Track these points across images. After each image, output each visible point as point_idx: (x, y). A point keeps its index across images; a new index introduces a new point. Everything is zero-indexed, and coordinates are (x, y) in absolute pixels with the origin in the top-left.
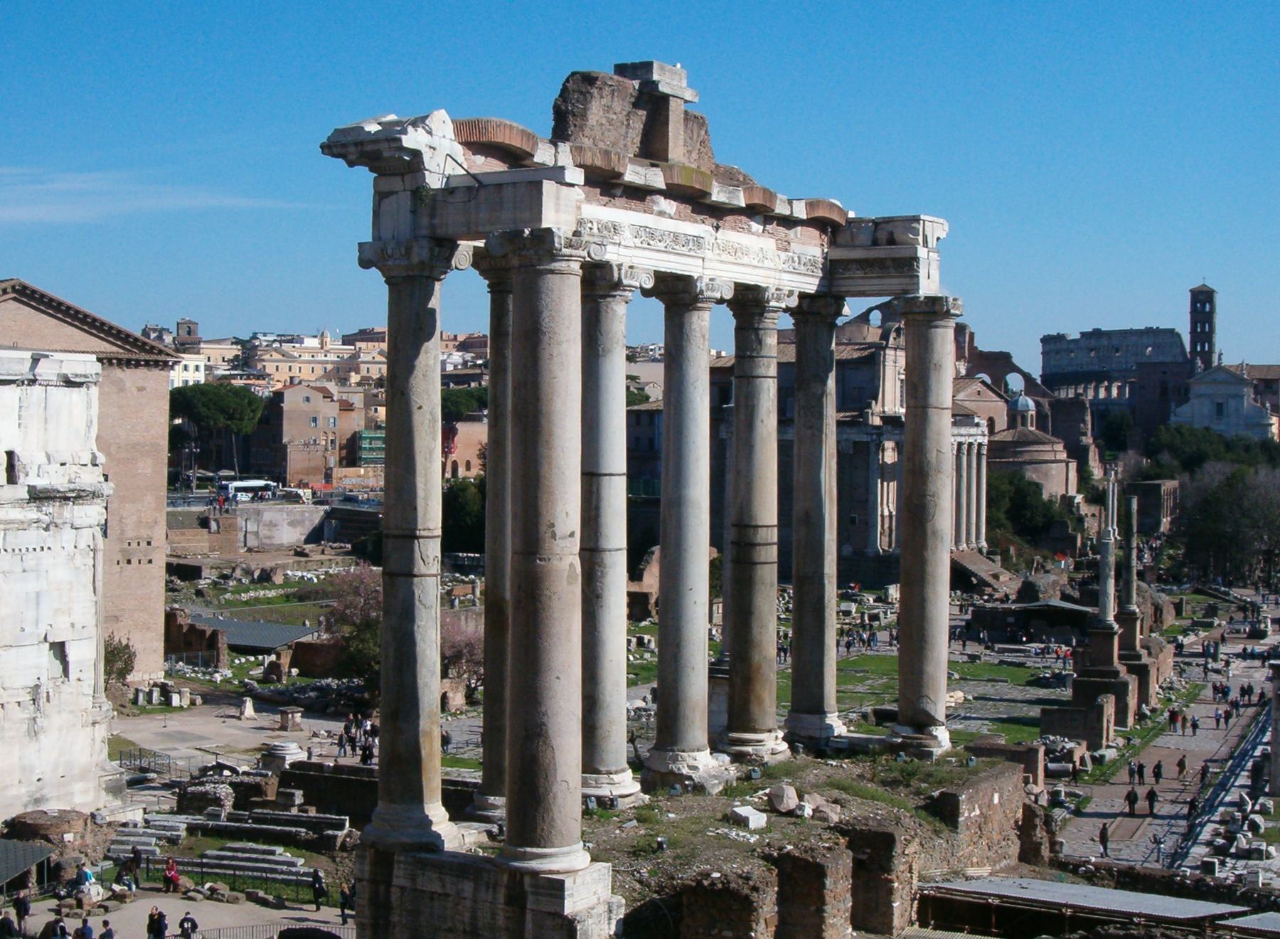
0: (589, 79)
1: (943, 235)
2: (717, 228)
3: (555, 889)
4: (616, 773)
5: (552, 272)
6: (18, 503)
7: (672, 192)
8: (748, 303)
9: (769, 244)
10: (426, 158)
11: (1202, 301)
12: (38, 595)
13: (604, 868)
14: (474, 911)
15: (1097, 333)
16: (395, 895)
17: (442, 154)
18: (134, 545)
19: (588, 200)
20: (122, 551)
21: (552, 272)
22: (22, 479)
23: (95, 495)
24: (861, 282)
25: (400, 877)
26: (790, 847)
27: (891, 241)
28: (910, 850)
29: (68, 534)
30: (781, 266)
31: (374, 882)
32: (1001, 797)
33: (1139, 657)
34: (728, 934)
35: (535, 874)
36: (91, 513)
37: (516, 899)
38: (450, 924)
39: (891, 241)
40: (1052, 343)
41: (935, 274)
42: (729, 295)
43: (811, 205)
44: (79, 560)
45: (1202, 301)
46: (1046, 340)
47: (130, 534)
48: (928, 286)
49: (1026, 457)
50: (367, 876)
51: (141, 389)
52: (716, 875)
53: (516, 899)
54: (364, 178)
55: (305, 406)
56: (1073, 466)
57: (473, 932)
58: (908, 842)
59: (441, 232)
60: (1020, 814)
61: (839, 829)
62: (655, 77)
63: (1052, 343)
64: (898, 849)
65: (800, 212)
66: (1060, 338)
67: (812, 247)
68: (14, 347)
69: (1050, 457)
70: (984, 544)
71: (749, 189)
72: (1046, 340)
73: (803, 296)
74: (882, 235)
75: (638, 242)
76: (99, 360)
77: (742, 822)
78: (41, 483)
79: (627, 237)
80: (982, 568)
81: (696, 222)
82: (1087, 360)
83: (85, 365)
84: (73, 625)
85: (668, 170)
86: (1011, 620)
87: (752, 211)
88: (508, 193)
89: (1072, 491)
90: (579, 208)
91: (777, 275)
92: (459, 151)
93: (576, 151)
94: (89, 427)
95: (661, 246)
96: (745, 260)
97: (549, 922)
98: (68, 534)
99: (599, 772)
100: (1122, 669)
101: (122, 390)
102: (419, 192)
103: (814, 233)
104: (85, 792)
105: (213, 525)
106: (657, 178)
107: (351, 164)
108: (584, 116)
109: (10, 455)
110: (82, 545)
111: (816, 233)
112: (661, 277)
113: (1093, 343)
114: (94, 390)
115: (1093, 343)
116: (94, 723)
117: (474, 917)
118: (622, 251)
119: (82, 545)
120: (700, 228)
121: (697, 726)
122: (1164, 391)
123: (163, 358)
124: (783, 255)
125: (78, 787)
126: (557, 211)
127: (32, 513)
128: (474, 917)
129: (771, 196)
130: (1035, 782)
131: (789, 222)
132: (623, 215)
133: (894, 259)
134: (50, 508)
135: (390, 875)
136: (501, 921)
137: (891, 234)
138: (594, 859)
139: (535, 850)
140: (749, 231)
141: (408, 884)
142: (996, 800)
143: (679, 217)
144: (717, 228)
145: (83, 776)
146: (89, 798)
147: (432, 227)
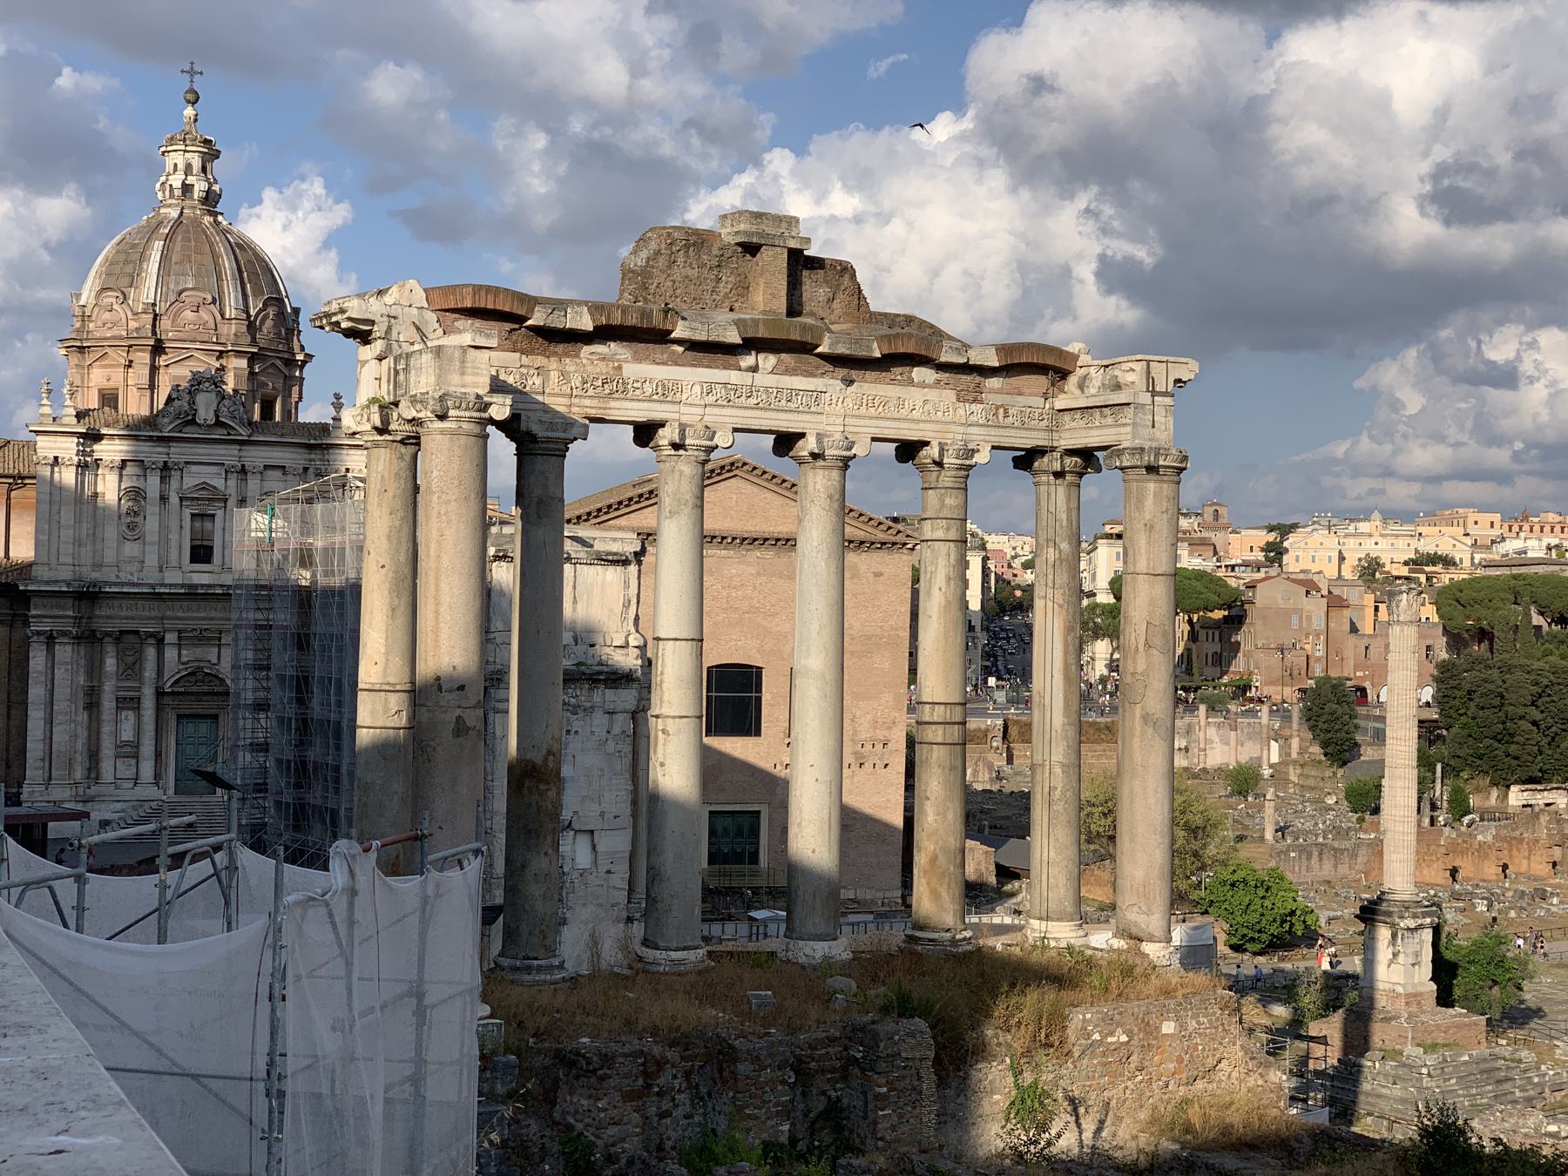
4: (676, 950)
7: (752, 344)
18: (868, 747)
19: (638, 359)
24: (1084, 433)
29: (599, 719)
32: (1182, 1026)
34: (585, 1102)
47: (864, 734)
51: (877, 575)
75: (711, 399)
81: (814, 376)
84: (602, 814)
90: (620, 368)
91: (961, 430)
95: (753, 401)
98: (599, 719)
106: (734, 337)
110: (616, 730)
116: (630, 920)
118: (684, 409)
119: (616, 730)
126: (463, 374)
140: (911, 382)
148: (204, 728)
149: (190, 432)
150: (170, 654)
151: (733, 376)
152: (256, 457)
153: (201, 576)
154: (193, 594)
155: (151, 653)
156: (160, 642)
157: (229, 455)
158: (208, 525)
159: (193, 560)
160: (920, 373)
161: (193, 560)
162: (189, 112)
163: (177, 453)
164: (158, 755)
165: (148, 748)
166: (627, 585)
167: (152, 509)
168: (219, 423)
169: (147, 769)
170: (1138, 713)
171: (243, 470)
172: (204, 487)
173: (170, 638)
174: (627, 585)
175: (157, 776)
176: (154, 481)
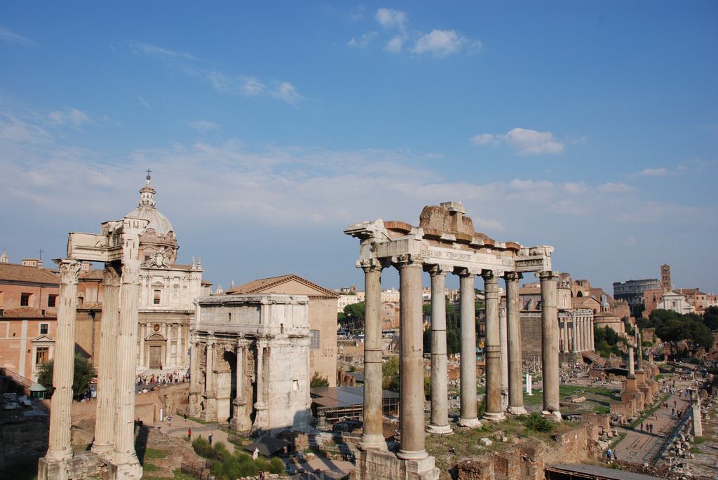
0: (431, 208)
1: (552, 252)
2: (475, 252)
3: (415, 465)
5: (412, 267)
6: (285, 339)
7: (458, 241)
8: (486, 275)
9: (494, 257)
10: (375, 234)
11: (665, 270)
12: (290, 366)
13: (432, 459)
14: (391, 470)
15: (631, 281)
16: (367, 464)
17: (379, 231)
19: (431, 245)
20: (324, 353)
21: (412, 267)
22: (285, 332)
23: (307, 336)
25: (368, 459)
26: (497, 453)
27: (535, 254)
28: (541, 454)
29: (299, 348)
30: (498, 264)
31: (360, 460)
33: (645, 386)
35: (408, 460)
36: (306, 342)
37: (403, 468)
38: (383, 475)
39: (535, 254)
40: (616, 285)
41: (550, 264)
42: (480, 273)
43: (507, 244)
44: (302, 356)
45: (665, 270)
46: (614, 284)
47: (327, 348)
48: (547, 266)
49: (607, 321)
50: (359, 457)
52: (469, 462)
53: (403, 468)
54: (357, 239)
55: (385, 310)
56: (623, 324)
57: (391, 478)
58: (540, 452)
59: (379, 256)
60: (586, 442)
61: (517, 446)
62: (452, 206)
63: (616, 285)
64: (536, 455)
65: (504, 246)
66: (619, 283)
67: (509, 257)
68: (284, 294)
69: (615, 321)
70: (594, 349)
71: (485, 240)
72: (614, 284)
73: (506, 273)
74: (532, 252)
76: (309, 297)
77: (483, 444)
78: (291, 333)
79: (444, 255)
80: (593, 357)
82: (627, 290)
83: (305, 299)
85: (456, 235)
86: (602, 373)
87: (487, 246)
88: (398, 243)
89: (623, 331)
90: (427, 248)
92: (386, 231)
93: (425, 230)
94: (306, 316)
96: (485, 262)
97: (414, 476)
98: (299, 348)
99: (438, 425)
100: (638, 390)
101: (324, 306)
102: (373, 244)
103: (510, 252)
104: (303, 425)
105: (357, 345)
106: (454, 238)
107: (354, 236)
108: (429, 220)
109: (282, 324)
111: (511, 252)
112: (455, 268)
113: (630, 285)
114: (307, 306)
115: (630, 285)
117: (390, 473)
120: (470, 252)
121: (471, 410)
122: (654, 300)
123: (335, 296)
124: (499, 260)
125: (301, 423)
127: (289, 342)
128: (390, 473)
129: (494, 241)
130: (607, 428)
131: (501, 250)
132: (444, 250)
133: (536, 260)
134: (294, 340)
135: (366, 457)
136: (399, 475)
137: (534, 252)
138: (429, 455)
139: (410, 452)
140: (487, 253)
141: (371, 461)
142: (576, 437)
143: (462, 249)
144: (475, 252)
145: (303, 420)
146: (305, 427)
147: (377, 255)
148: (157, 349)
149: (155, 267)
150: (148, 329)
151: (452, 250)
152: (172, 274)
153: (157, 307)
154: (155, 312)
155: (143, 329)
156: (146, 325)
157: (165, 274)
158: (159, 293)
159: (155, 303)
160: (489, 250)
161: (155, 303)
162: (148, 181)
163: (151, 273)
164: (145, 357)
165: (142, 356)
166: (305, 310)
167: (144, 289)
168: (163, 265)
169: (142, 361)
170: (551, 347)
171: (168, 278)
172: (158, 283)
173: (148, 325)
174: (305, 310)
175: (145, 364)
176: (144, 280)
